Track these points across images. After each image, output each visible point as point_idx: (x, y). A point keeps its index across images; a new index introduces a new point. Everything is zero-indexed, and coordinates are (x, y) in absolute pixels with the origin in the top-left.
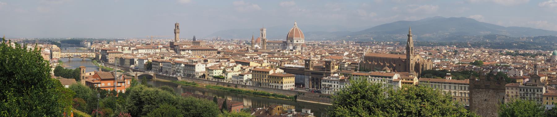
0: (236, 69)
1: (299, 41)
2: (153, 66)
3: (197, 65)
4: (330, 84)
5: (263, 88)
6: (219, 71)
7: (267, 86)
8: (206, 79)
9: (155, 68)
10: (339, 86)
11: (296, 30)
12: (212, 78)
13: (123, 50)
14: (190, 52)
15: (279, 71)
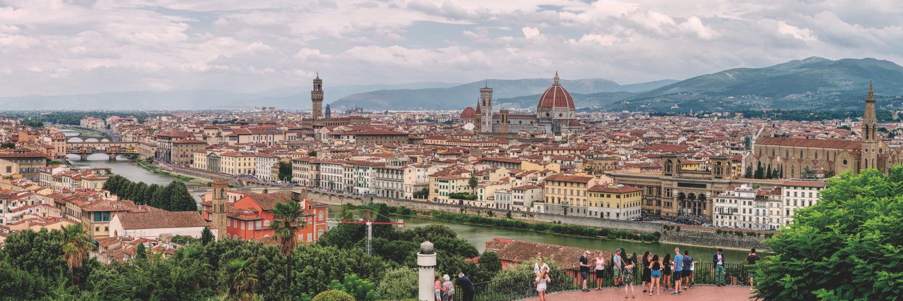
0: (493, 177)
1: (564, 114)
2: (294, 172)
3: (406, 171)
4: (734, 206)
5: (572, 217)
6: (460, 182)
7: (581, 214)
8: (431, 198)
9: (301, 176)
10: (754, 211)
11: (559, 91)
12: (447, 198)
13: (205, 138)
14: (352, 140)
15: (604, 180)
